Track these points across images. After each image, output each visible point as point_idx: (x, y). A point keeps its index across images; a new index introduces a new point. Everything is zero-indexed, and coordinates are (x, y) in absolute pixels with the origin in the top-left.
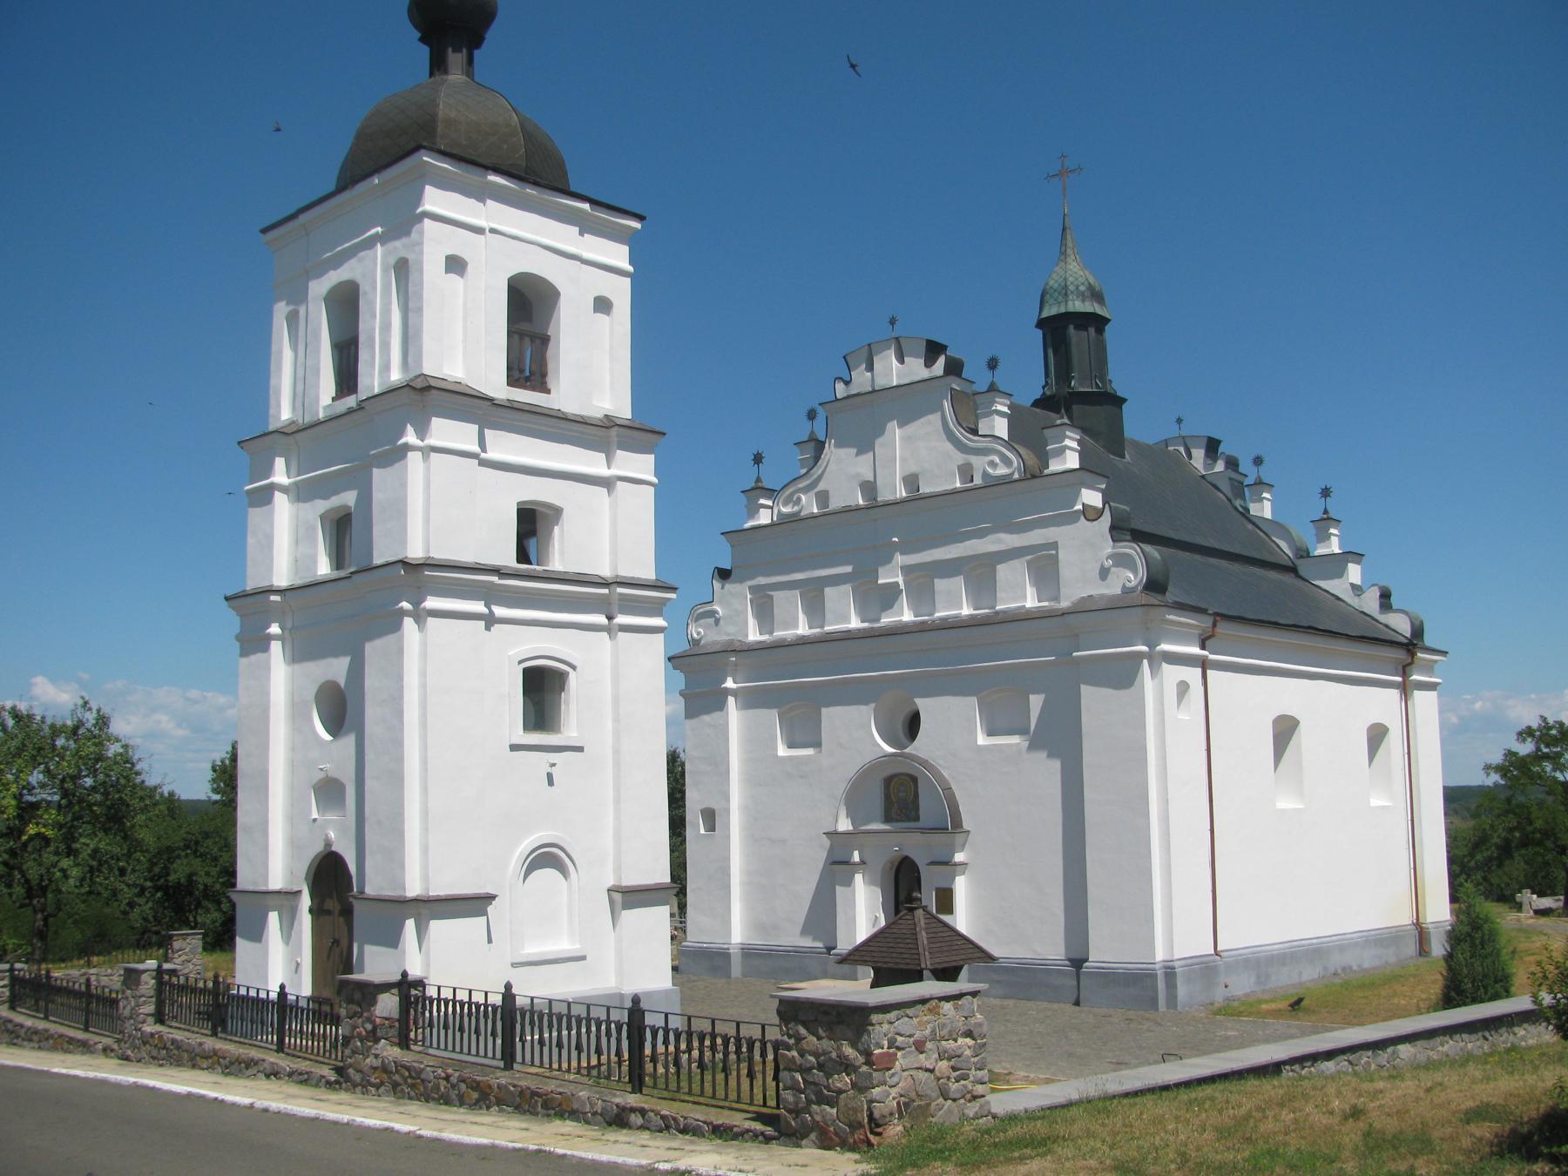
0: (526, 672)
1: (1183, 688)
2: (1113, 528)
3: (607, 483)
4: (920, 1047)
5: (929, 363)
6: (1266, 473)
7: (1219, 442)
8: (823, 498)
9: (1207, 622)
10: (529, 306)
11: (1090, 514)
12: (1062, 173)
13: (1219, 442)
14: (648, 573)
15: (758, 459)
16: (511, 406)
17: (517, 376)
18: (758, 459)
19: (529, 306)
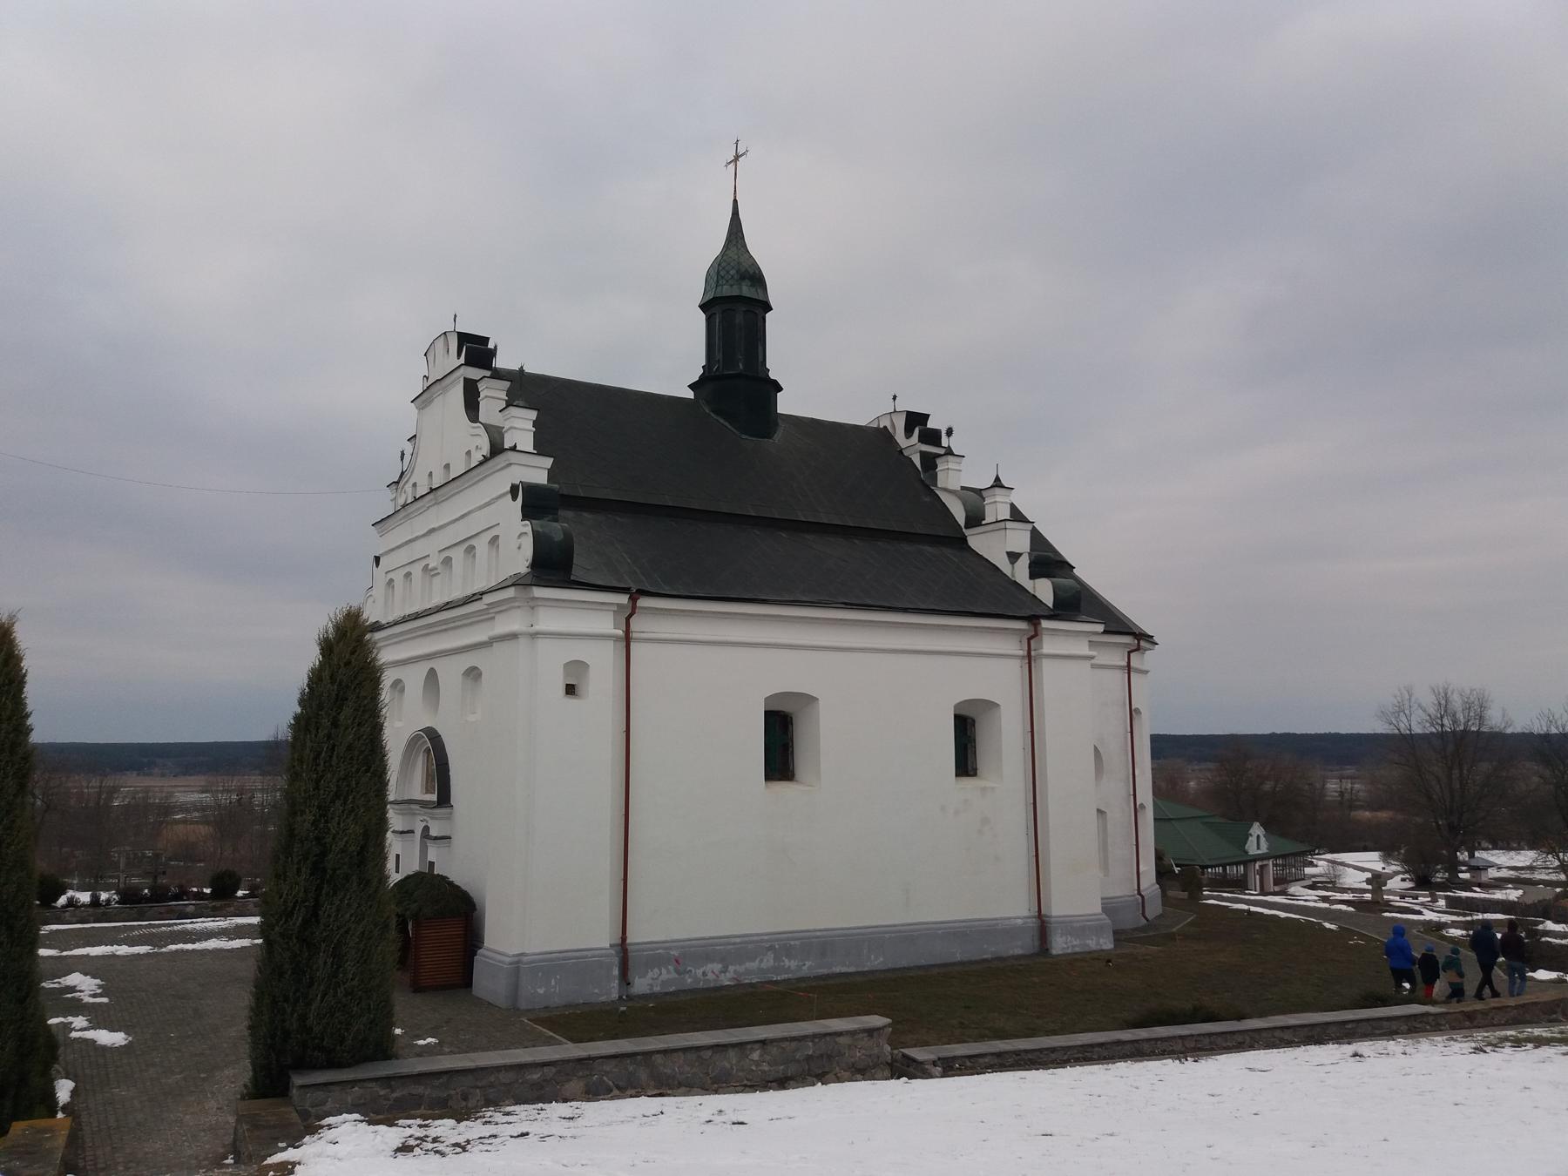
2: (523, 507)
5: (459, 356)
6: (955, 443)
8: (415, 485)
9: (623, 599)
12: (737, 157)
18: (403, 454)
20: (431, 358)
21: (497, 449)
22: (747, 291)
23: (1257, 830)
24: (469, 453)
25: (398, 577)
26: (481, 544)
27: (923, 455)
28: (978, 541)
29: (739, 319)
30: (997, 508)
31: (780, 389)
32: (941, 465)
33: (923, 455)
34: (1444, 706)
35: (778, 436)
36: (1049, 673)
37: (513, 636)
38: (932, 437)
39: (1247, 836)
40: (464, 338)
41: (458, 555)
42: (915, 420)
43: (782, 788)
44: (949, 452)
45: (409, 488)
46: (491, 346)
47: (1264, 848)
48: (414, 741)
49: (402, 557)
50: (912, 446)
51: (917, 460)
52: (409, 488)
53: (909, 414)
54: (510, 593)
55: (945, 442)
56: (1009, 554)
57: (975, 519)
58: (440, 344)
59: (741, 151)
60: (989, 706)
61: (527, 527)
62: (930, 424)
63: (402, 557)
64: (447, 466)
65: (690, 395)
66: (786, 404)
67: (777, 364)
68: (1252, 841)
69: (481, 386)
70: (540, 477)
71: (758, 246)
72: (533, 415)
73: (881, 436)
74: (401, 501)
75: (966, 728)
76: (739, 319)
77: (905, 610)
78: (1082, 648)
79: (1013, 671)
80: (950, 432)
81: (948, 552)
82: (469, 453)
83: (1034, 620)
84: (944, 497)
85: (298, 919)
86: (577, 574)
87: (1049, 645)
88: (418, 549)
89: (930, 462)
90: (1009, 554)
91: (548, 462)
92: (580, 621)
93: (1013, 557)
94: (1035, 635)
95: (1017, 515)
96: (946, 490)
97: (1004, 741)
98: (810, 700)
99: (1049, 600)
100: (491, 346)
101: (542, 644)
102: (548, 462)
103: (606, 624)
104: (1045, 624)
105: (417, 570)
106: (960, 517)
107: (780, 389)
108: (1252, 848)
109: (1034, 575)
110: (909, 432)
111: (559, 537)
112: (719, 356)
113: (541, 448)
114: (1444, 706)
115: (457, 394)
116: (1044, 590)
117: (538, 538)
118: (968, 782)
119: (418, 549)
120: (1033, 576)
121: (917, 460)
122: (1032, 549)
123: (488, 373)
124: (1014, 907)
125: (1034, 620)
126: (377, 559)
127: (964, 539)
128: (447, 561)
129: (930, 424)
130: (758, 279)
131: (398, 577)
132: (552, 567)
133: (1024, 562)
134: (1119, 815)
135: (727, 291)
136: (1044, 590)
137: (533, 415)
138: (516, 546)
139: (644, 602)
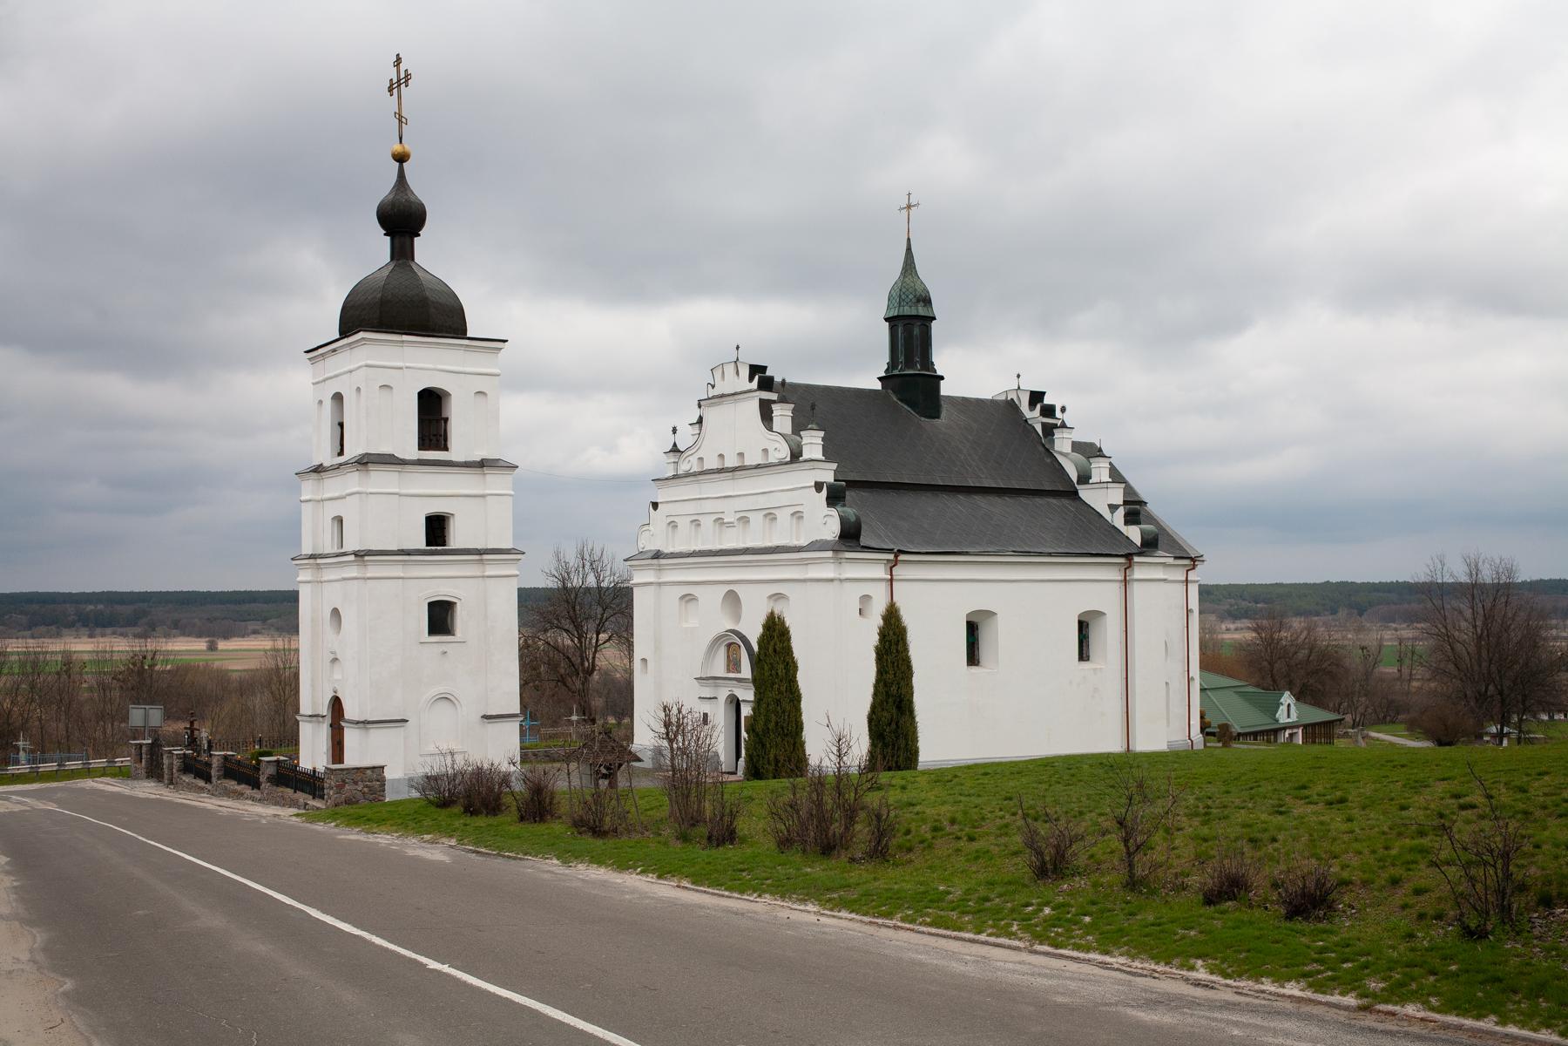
0: (431, 605)
1: (866, 599)
3: (483, 496)
4: (356, 783)
5: (751, 379)
7: (1043, 394)
8: (701, 459)
9: (891, 557)
10: (432, 405)
11: (818, 486)
12: (909, 207)
13: (1043, 394)
14: (510, 546)
15: (674, 430)
16: (421, 463)
17: (424, 444)
18: (674, 430)
19: (432, 405)
20: (718, 374)
21: (796, 455)
22: (922, 311)
23: (1287, 698)
24: (765, 451)
25: (684, 523)
26: (783, 516)
27: (1044, 425)
28: (1085, 493)
29: (916, 331)
30: (1100, 471)
31: (942, 378)
32: (1058, 434)
33: (1044, 425)
34: (1474, 569)
35: (944, 414)
36: (1137, 590)
37: (832, 580)
38: (1049, 411)
39: (1279, 705)
40: (756, 370)
41: (757, 519)
42: (1036, 397)
43: (974, 669)
44: (1064, 426)
45: (694, 459)
46: (768, 373)
47: (1294, 718)
48: (718, 639)
49: (691, 508)
50: (1033, 416)
51: (1039, 429)
52: (694, 459)
53: (1032, 393)
54: (830, 554)
55: (1058, 414)
56: (1111, 506)
57: (1085, 478)
58: (730, 369)
59: (913, 202)
60: (1099, 614)
61: (833, 512)
62: (1047, 401)
63: (691, 508)
64: (741, 455)
65: (878, 386)
66: (946, 389)
67: (942, 361)
68: (1283, 710)
69: (774, 407)
70: (828, 476)
71: (928, 275)
72: (822, 434)
73: (1011, 406)
74: (684, 467)
75: (1083, 627)
76: (916, 331)
77: (1050, 555)
78: (1159, 574)
79: (1115, 590)
80: (1063, 410)
81: (1066, 502)
82: (765, 451)
83: (1129, 556)
84: (1061, 459)
85: (894, 726)
86: (864, 541)
87: (1138, 573)
88: (708, 506)
89: (1049, 430)
90: (1111, 506)
91: (835, 466)
92: (869, 569)
93: (1113, 508)
94: (1129, 566)
95: (1116, 476)
96: (1061, 453)
97: (1107, 637)
98: (990, 614)
99: (1137, 540)
100: (768, 373)
101: (847, 585)
102: (835, 466)
103: (880, 572)
104: (1136, 559)
105: (707, 522)
106: (1074, 476)
107: (942, 378)
108: (1282, 717)
109: (1127, 523)
110: (1032, 404)
111: (853, 519)
112: (902, 359)
113: (829, 453)
114: (1474, 569)
115: (752, 407)
116: (1134, 534)
117: (844, 521)
118: (1085, 665)
119: (708, 506)
120: (1127, 523)
121: (1039, 429)
122: (1125, 503)
123: (773, 396)
124: (1114, 746)
125: (1129, 556)
126: (655, 505)
127: (1076, 493)
128: (744, 520)
129: (1047, 401)
130: (927, 301)
131: (684, 523)
132: (850, 536)
133: (1121, 512)
134: (1179, 684)
135: (907, 311)
136: (1134, 534)
137: (822, 434)
138: (828, 524)
139: (902, 557)
